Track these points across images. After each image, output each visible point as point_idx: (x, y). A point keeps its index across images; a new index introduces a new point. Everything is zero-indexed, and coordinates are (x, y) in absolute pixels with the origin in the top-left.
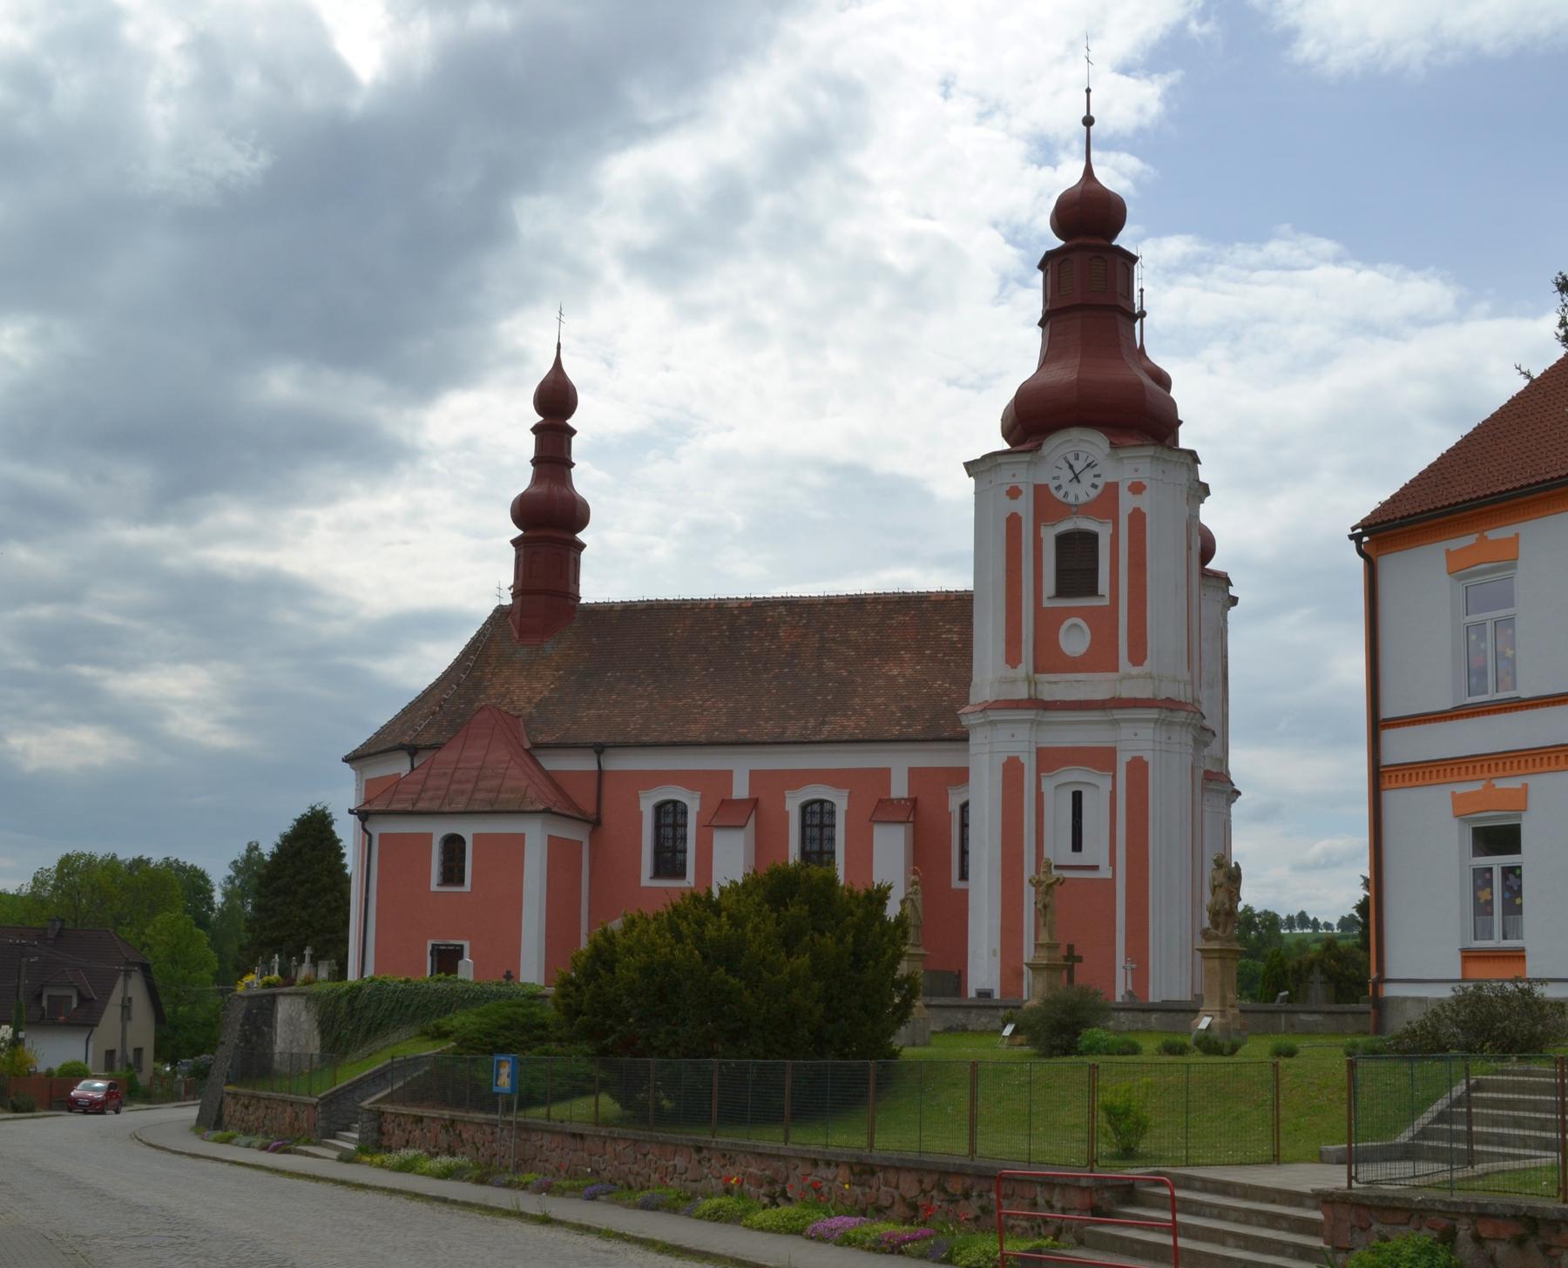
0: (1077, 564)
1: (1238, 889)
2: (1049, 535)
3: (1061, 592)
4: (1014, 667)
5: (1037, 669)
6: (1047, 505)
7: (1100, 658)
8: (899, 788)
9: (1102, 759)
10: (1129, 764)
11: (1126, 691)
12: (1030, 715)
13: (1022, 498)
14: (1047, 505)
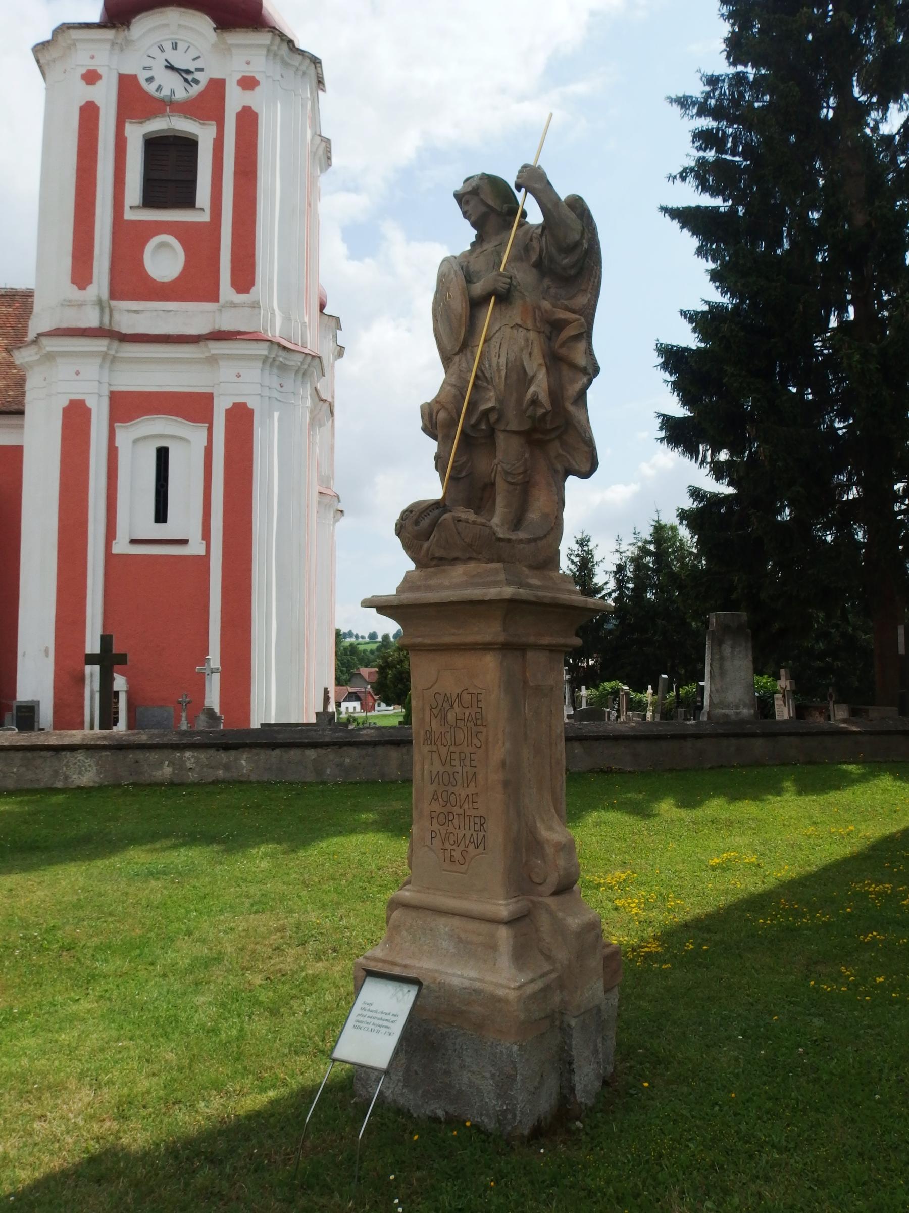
0: (170, 170)
1: (588, 314)
2: (136, 134)
3: (150, 200)
5: (116, 293)
6: (133, 99)
7: (197, 284)
9: (195, 407)
10: (228, 412)
11: (227, 323)
12: (100, 345)
13: (100, 84)
14: (133, 99)
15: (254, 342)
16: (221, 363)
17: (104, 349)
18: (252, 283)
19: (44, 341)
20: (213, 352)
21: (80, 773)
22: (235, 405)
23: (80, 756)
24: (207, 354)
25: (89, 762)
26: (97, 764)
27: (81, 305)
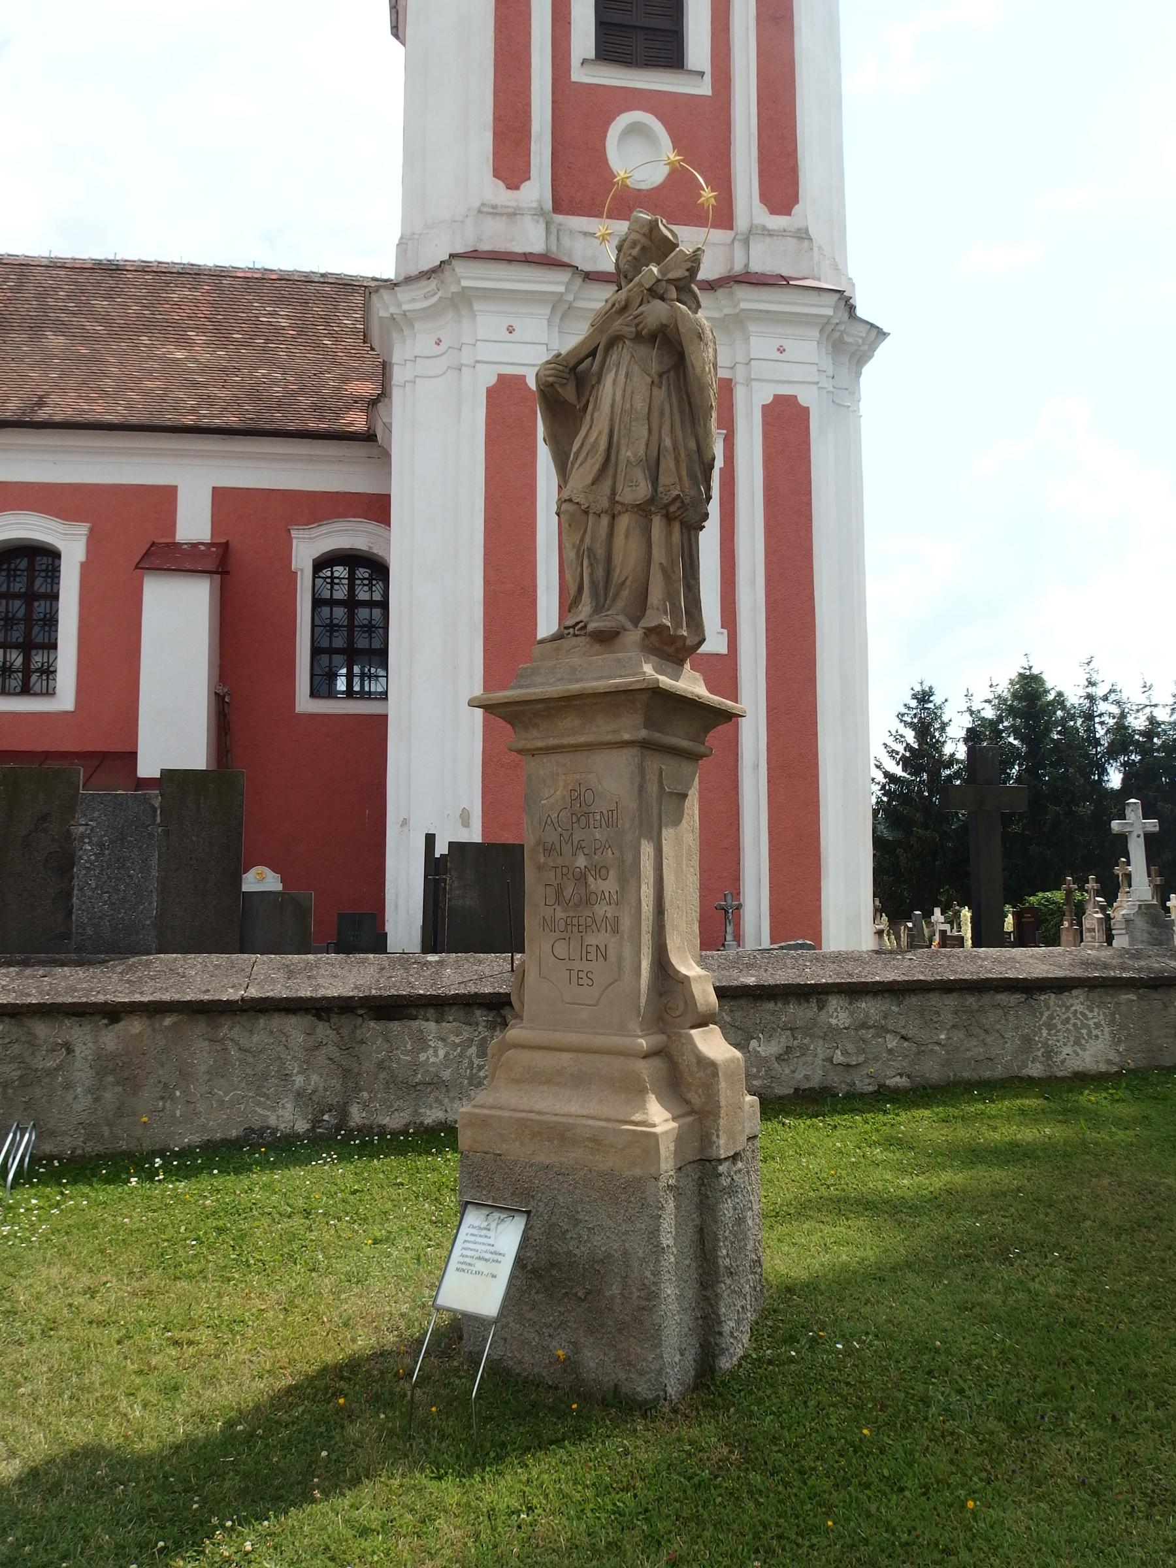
4: (513, 186)
5: (564, 202)
8: (194, 524)
11: (762, 260)
15: (816, 293)
16: (752, 328)
17: (562, 289)
18: (794, 199)
19: (460, 267)
20: (744, 305)
21: (1077, 1043)
22: (777, 398)
23: (1077, 1001)
24: (727, 311)
25: (1096, 1016)
26: (1112, 1022)
27: (515, 214)
